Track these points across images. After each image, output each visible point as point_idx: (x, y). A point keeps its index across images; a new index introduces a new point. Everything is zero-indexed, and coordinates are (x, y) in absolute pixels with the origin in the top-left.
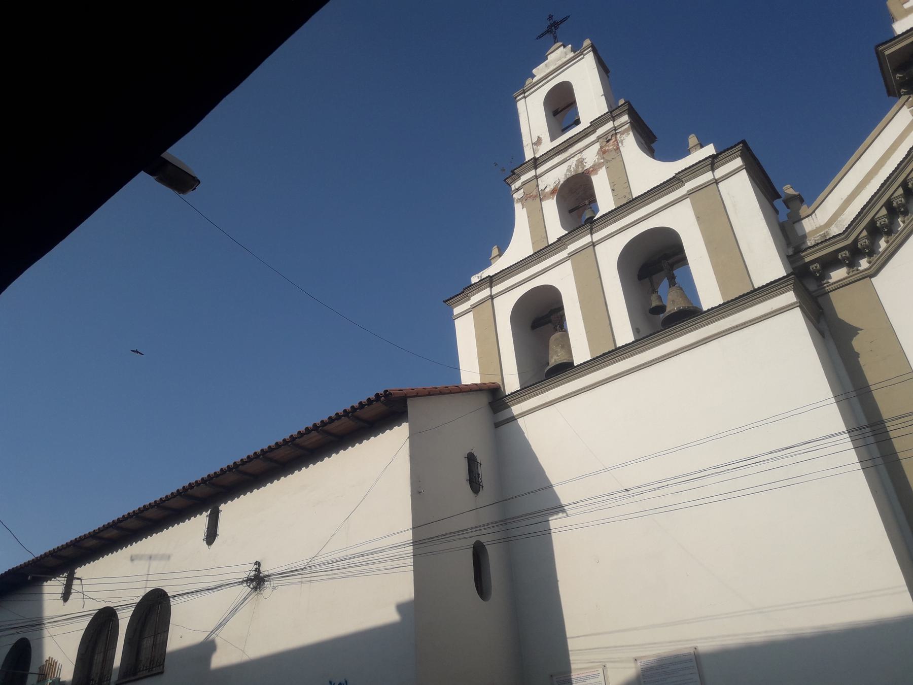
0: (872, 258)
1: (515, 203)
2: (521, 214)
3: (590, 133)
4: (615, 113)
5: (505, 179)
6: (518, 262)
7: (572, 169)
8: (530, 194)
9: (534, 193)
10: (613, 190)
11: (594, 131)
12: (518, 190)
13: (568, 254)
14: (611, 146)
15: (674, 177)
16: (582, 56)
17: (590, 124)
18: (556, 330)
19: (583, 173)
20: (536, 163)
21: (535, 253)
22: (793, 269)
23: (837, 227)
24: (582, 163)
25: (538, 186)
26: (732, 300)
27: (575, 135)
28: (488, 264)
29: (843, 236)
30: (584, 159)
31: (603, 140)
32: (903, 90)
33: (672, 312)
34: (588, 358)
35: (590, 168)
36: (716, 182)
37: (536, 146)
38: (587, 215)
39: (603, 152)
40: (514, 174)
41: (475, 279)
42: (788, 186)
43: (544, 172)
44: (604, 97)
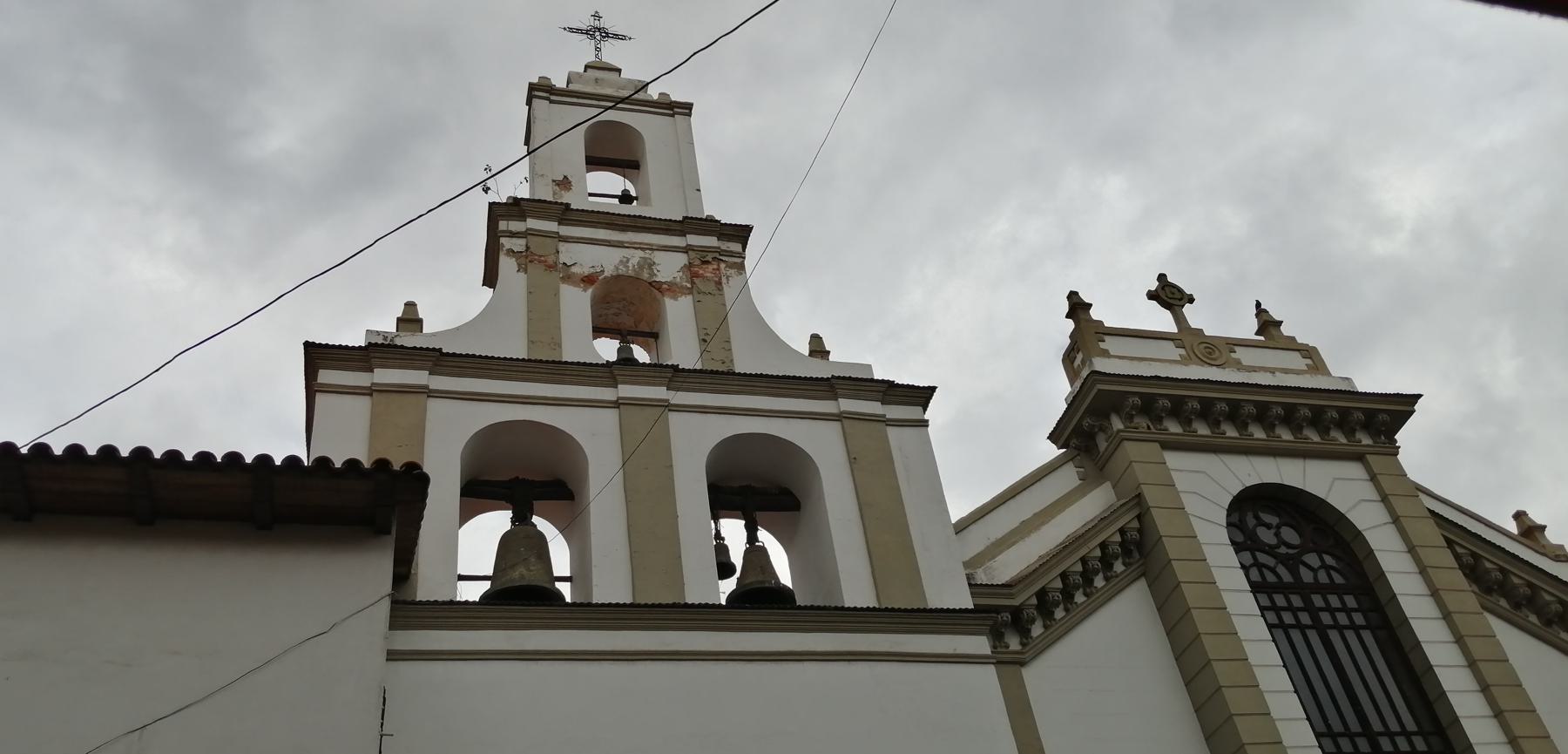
1: (501, 253)
3: (675, 230)
6: (511, 359)
8: (541, 256)
9: (551, 260)
10: (705, 341)
11: (683, 234)
14: (708, 271)
19: (650, 283)
22: (974, 605)
23: (985, 572)
26: (906, 610)
27: (650, 218)
30: (654, 263)
32: (1074, 441)
33: (767, 585)
35: (665, 283)
37: (557, 188)
43: (578, 238)
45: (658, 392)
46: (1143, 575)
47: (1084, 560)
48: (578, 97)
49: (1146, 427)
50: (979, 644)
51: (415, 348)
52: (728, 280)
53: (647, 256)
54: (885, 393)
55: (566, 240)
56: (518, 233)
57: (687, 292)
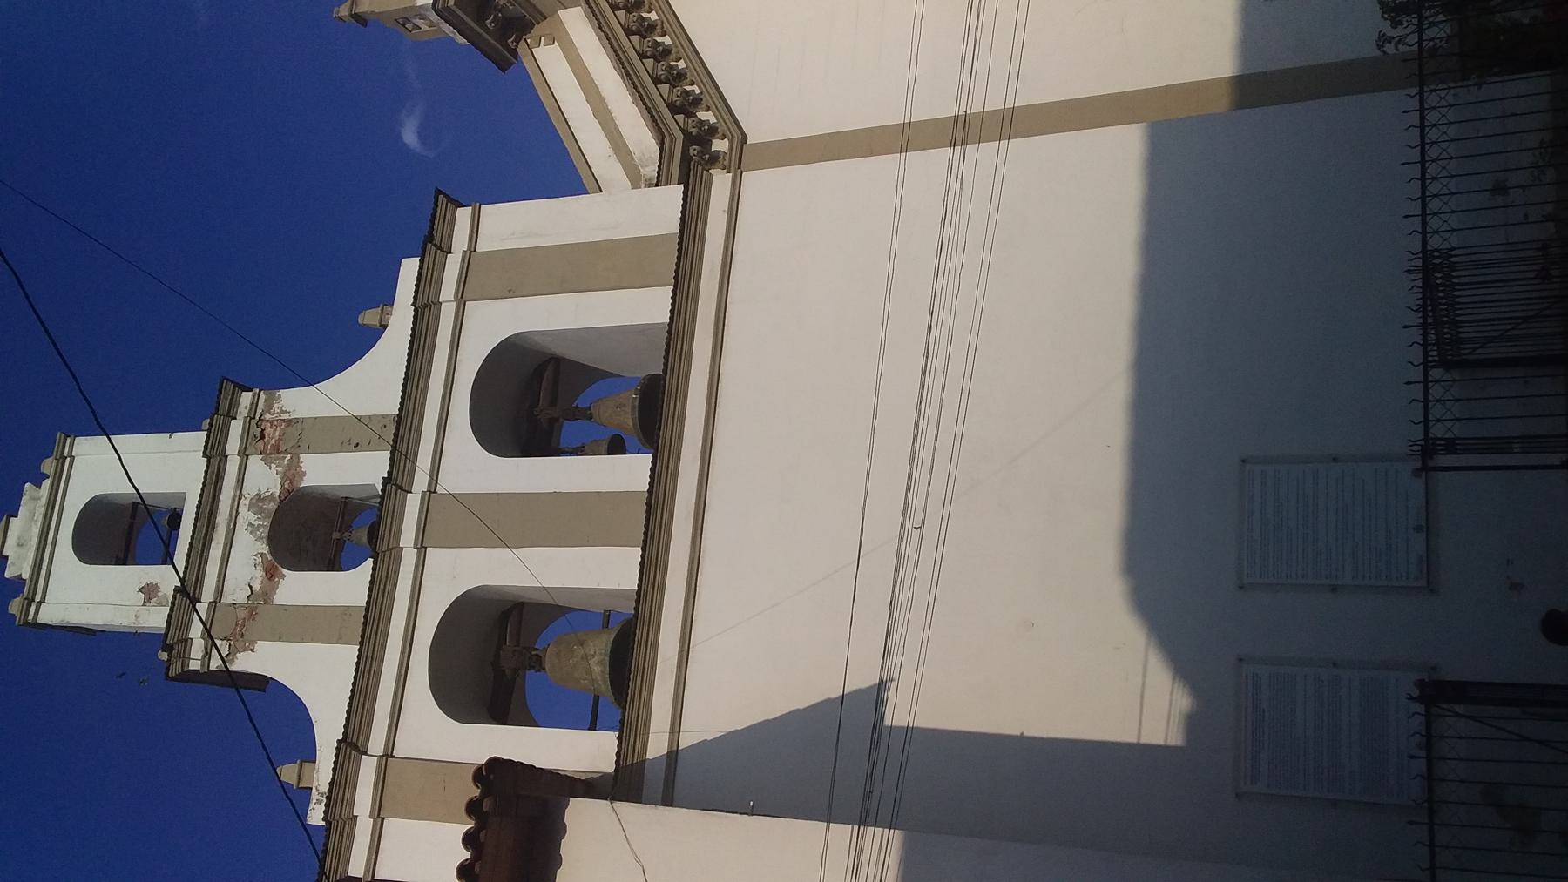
0: (719, 130)
2: (260, 659)
3: (219, 469)
5: (167, 674)
7: (257, 522)
8: (237, 625)
9: (243, 613)
11: (224, 458)
14: (273, 434)
15: (416, 311)
16: (68, 459)
17: (206, 459)
19: (281, 501)
21: (361, 644)
23: (646, 166)
26: (679, 258)
27: (201, 495)
29: (668, 138)
33: (637, 403)
39: (271, 454)
41: (316, 816)
43: (218, 581)
45: (413, 504)
48: (40, 568)
50: (720, 182)
51: (334, 770)
52: (286, 412)
53: (247, 502)
54: (439, 248)
55: (219, 592)
56: (206, 648)
57: (296, 461)
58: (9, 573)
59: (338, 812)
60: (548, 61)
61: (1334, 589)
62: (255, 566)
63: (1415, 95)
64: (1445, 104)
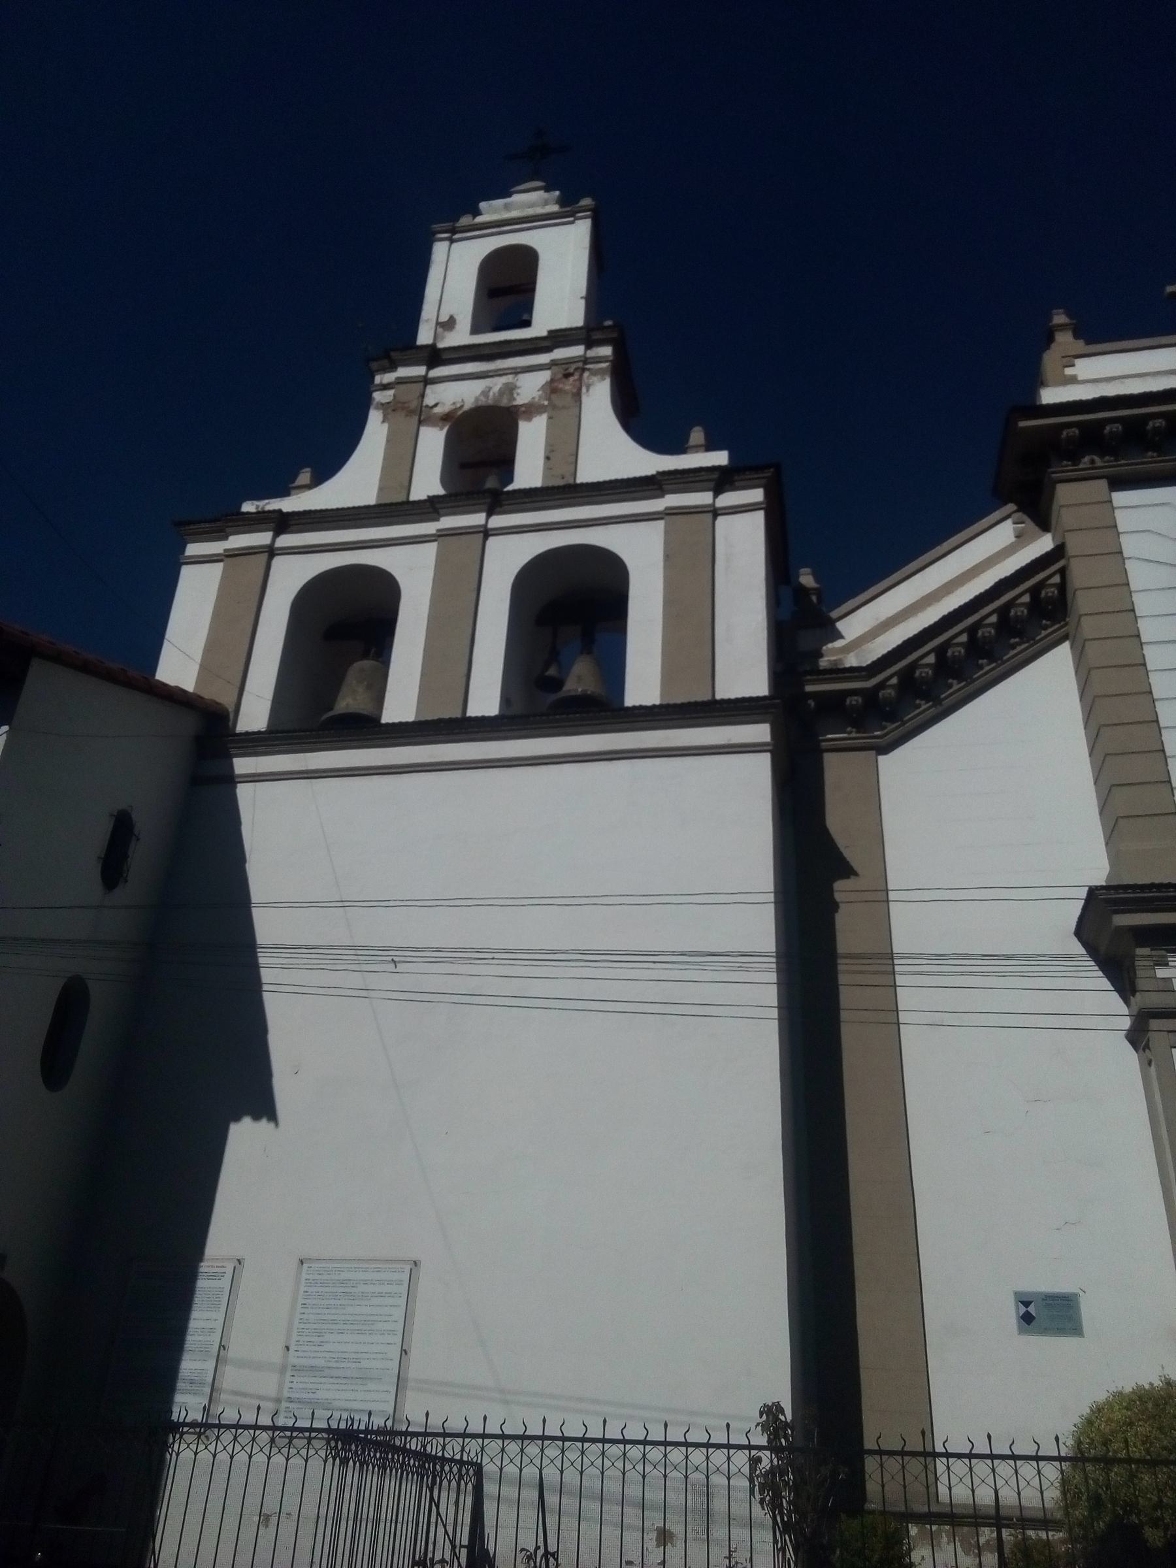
4: (597, 336)
8: (404, 403)
9: (414, 405)
10: (547, 458)
11: (548, 349)
12: (385, 387)
13: (438, 530)
14: (568, 385)
15: (653, 476)
16: (571, 219)
18: (365, 655)
20: (435, 356)
24: (512, 394)
25: (423, 396)
28: (285, 492)
30: (516, 386)
31: (559, 371)
33: (573, 693)
34: (409, 716)
35: (522, 406)
36: (715, 513)
37: (440, 330)
38: (491, 483)
39: (551, 388)
40: (388, 357)
41: (248, 507)
42: (808, 570)
44: (582, 303)
46: (1065, 638)
47: (972, 630)
49: (1088, 463)
52: (588, 390)
58: (483, 205)
59: (230, 524)
60: (1002, 534)
61: (288, 1348)
62: (454, 403)
63: (502, 1430)
64: (647, 1470)
